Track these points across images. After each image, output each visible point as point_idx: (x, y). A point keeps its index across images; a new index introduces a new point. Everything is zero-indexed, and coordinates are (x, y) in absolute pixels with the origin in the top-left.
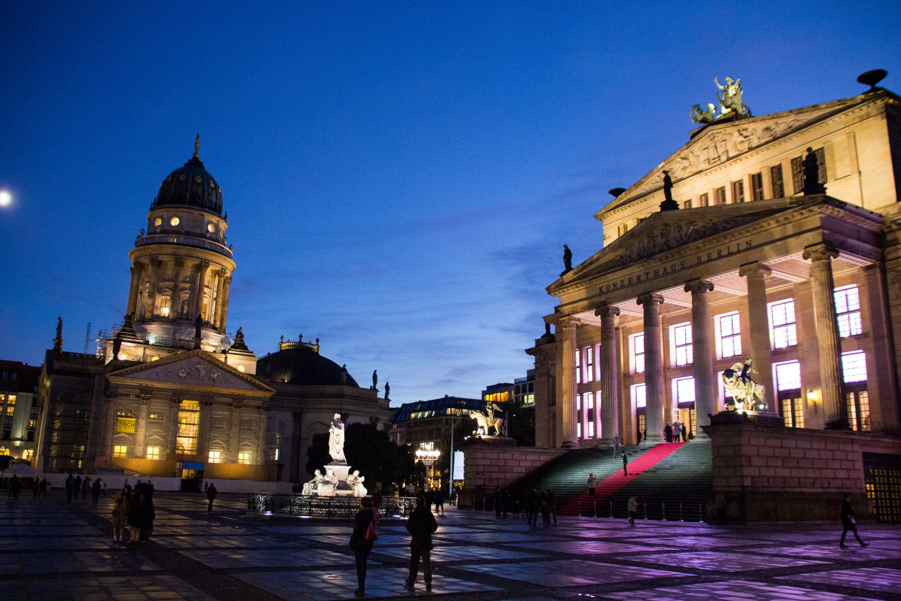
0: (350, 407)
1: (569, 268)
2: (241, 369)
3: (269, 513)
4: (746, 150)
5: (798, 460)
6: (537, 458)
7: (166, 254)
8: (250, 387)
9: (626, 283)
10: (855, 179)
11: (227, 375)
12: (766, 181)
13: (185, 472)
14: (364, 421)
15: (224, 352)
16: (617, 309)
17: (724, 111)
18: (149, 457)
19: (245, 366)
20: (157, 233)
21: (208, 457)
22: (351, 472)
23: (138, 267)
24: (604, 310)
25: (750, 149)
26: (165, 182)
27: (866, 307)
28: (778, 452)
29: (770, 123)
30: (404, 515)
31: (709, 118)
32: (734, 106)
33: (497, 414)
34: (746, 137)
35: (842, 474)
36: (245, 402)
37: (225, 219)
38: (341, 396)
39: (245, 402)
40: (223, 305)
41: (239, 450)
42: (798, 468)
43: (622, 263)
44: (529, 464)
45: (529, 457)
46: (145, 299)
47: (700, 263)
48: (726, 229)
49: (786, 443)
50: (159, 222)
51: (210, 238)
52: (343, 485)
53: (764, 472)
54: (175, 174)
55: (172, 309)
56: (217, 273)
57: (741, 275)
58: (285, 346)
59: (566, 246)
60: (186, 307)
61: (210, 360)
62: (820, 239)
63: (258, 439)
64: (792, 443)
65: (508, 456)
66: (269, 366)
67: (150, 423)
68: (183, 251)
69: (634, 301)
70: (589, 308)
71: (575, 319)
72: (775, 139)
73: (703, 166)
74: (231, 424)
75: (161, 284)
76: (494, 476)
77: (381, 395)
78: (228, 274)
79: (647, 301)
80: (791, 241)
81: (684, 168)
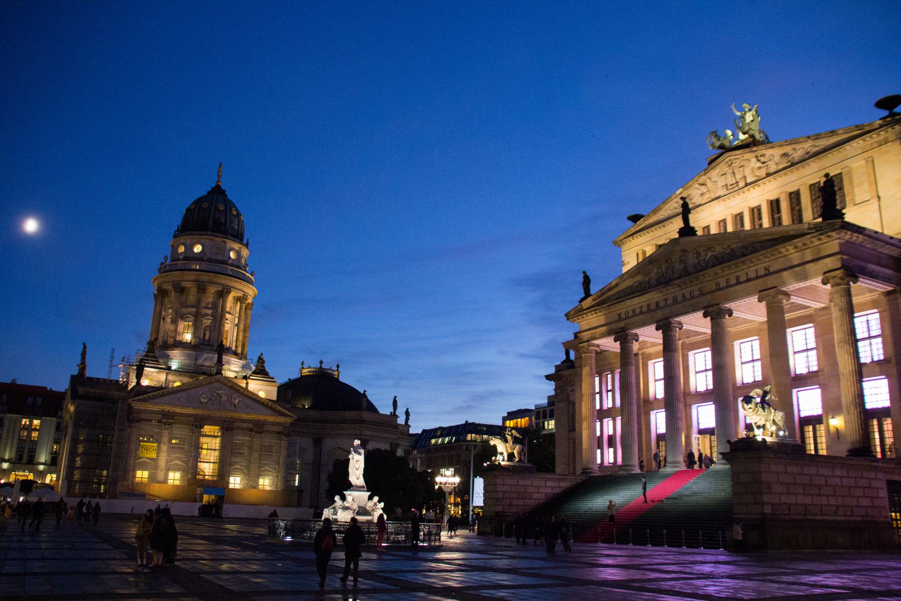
0: (369, 433)
1: (588, 294)
2: (262, 395)
3: (289, 539)
4: (764, 175)
5: (819, 487)
6: (556, 484)
7: (188, 280)
8: (270, 412)
9: (645, 309)
10: (874, 204)
11: (248, 401)
12: (784, 206)
13: (206, 497)
14: (384, 446)
15: (245, 378)
16: (636, 335)
17: (742, 137)
18: (170, 482)
19: (266, 391)
20: (179, 260)
21: (228, 483)
22: (370, 498)
23: (162, 293)
24: (623, 336)
25: (768, 175)
26: (188, 210)
27: (888, 332)
28: (799, 479)
29: (788, 149)
30: (423, 541)
31: (727, 144)
32: (751, 132)
33: (516, 441)
34: (763, 163)
35: (865, 502)
36: (266, 428)
37: (247, 245)
38: (362, 421)
39: (266, 428)
40: (245, 331)
41: (259, 475)
42: (820, 495)
43: (640, 289)
44: (549, 491)
45: (549, 484)
46: (167, 326)
47: (719, 289)
48: (744, 255)
49: (806, 470)
50: (182, 249)
51: (232, 265)
52: (363, 511)
53: (784, 499)
54: (198, 202)
55: (195, 335)
56: (240, 300)
57: (760, 301)
58: (305, 372)
59: (584, 273)
60: (208, 333)
61: (231, 385)
62: (839, 265)
63: (278, 464)
64: (812, 470)
65: (529, 482)
66: (290, 391)
67: (172, 448)
68: (205, 277)
69: (653, 327)
70: (608, 334)
71: (594, 345)
72: (793, 164)
74: (251, 448)
75: (184, 310)
76: (515, 502)
77: (401, 421)
78: (250, 301)
79: (666, 327)
80: (810, 267)
81: (702, 194)
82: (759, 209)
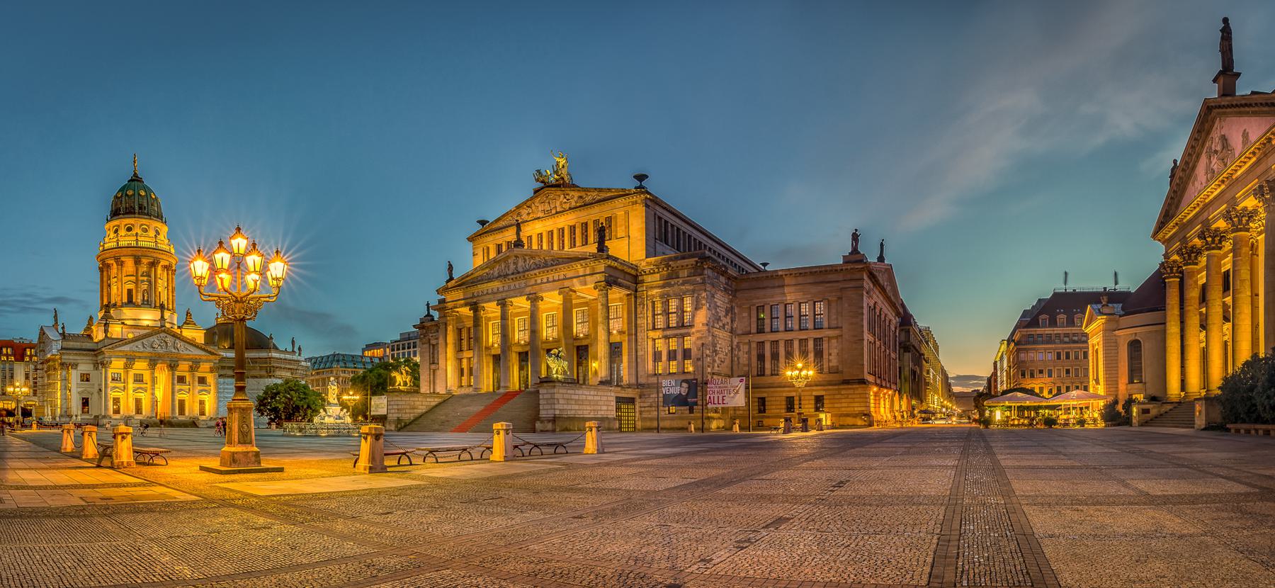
10: (626, 241)
24: (475, 307)
29: (583, 194)
70: (466, 305)
73: (541, 215)
79: (503, 304)
82: (563, 229)
